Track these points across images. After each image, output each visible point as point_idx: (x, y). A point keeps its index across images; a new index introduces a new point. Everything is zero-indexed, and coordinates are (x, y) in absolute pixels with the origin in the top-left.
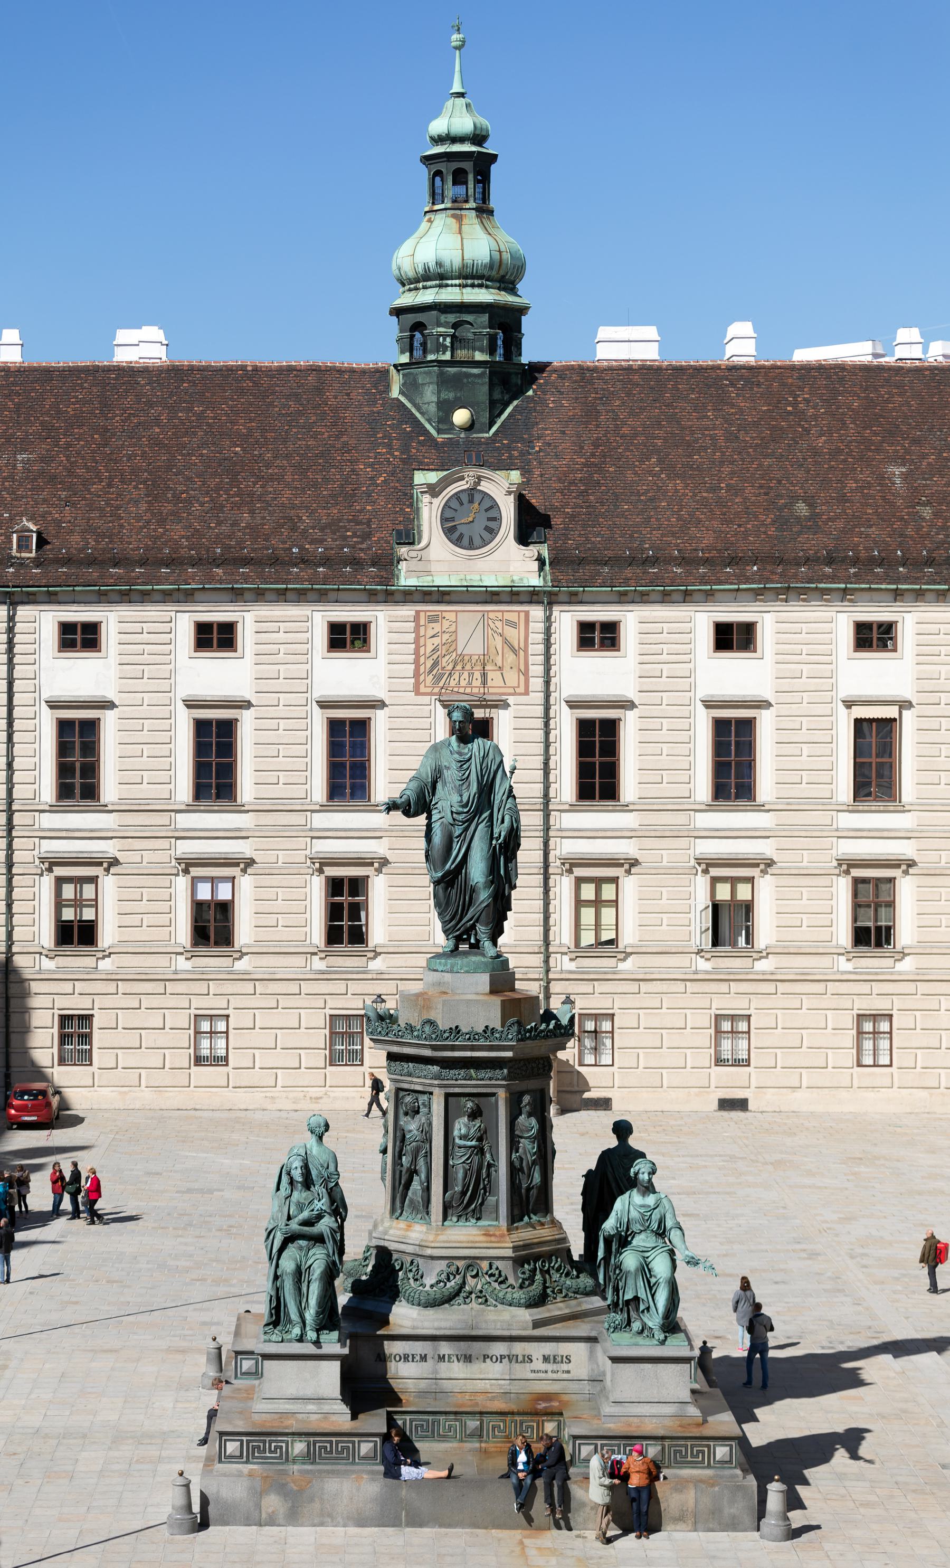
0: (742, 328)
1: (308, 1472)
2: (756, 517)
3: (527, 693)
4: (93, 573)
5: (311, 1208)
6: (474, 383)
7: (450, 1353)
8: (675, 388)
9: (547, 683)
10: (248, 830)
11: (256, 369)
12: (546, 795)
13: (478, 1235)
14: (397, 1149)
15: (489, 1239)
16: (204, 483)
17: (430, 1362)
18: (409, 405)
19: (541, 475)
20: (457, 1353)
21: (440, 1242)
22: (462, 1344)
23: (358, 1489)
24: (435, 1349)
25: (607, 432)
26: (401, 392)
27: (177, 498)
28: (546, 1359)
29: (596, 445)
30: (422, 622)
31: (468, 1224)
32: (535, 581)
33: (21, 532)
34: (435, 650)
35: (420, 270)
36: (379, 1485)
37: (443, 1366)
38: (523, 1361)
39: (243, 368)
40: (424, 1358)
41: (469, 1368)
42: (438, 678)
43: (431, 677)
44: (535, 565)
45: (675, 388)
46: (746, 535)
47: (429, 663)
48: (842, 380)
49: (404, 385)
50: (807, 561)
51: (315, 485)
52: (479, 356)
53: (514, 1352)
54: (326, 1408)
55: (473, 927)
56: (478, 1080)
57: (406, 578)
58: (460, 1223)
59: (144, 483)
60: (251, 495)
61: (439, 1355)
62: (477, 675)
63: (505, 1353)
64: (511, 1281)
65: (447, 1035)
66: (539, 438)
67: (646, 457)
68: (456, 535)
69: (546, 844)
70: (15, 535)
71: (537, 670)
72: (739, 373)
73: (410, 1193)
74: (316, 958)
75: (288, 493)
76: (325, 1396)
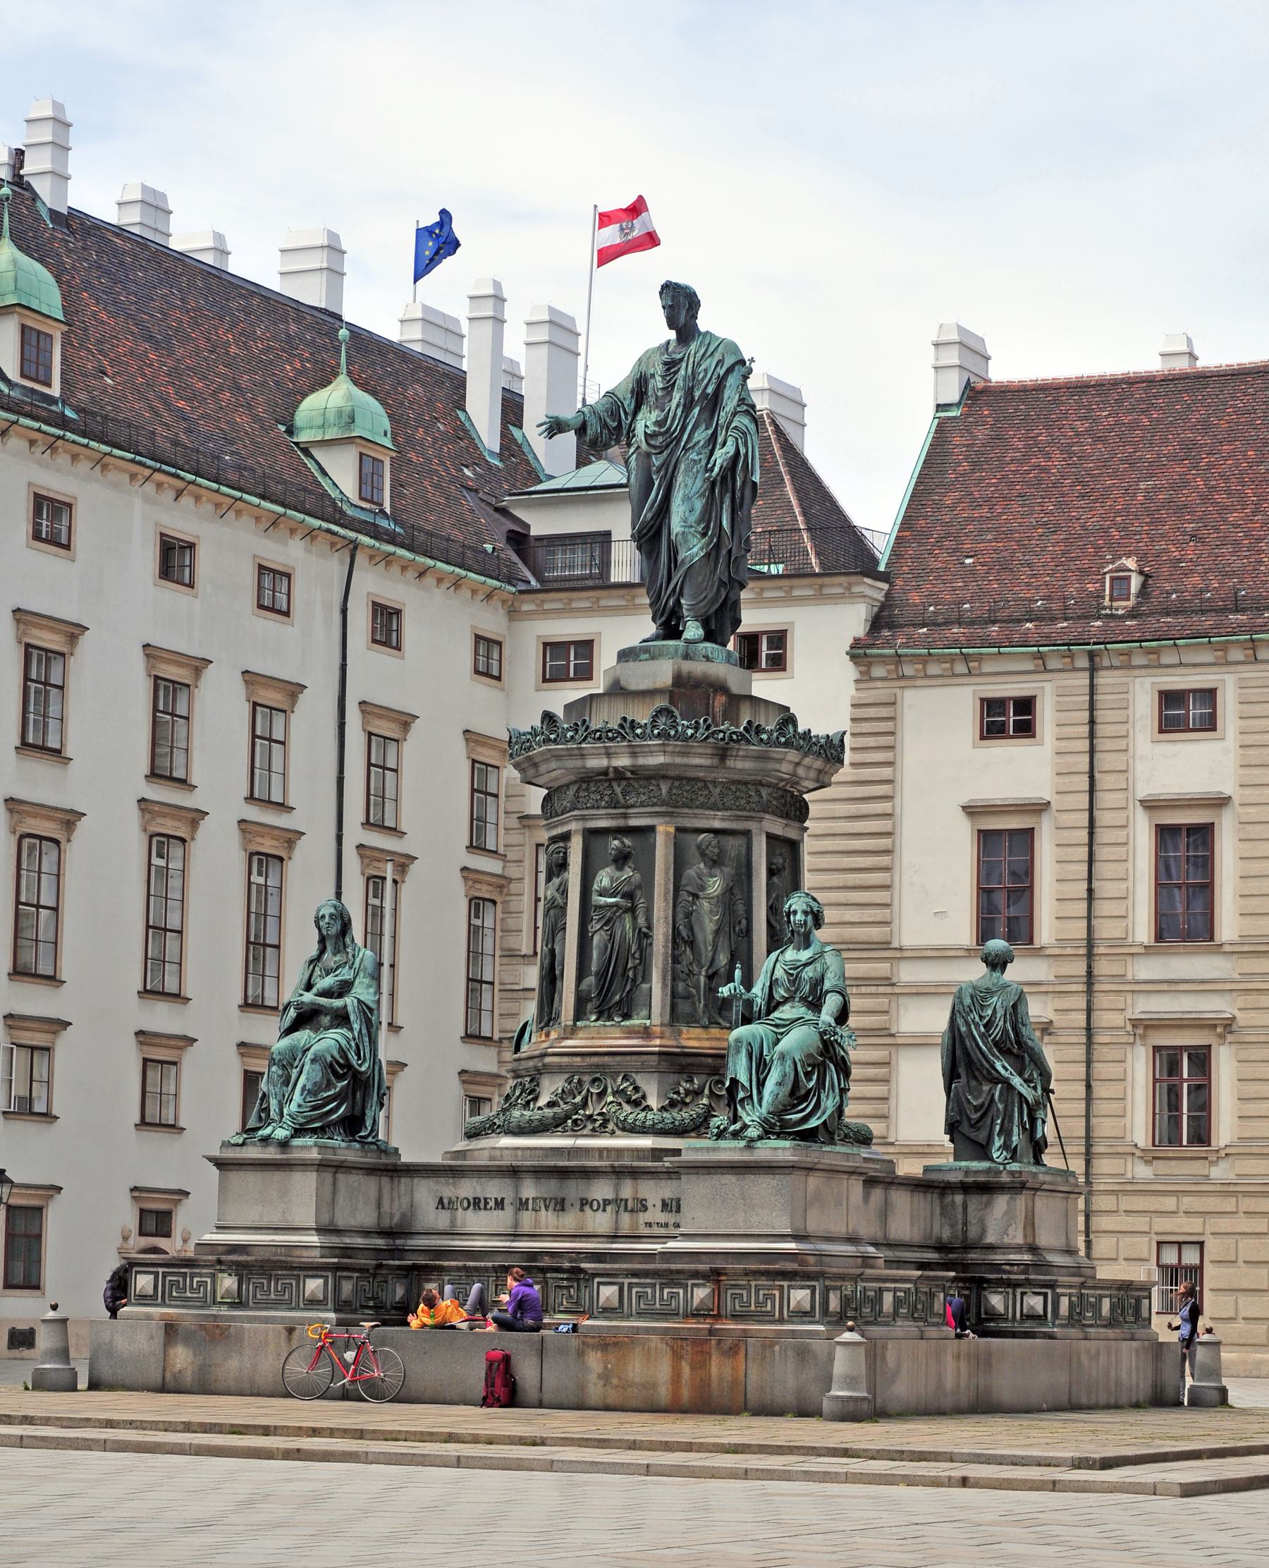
4: (1208, 621)
20: (545, 1196)
24: (517, 1191)
31: (608, 1023)
33: (1116, 571)
40: (500, 1204)
41: (561, 1219)
55: (678, 603)
58: (600, 1022)
61: (520, 1199)
63: (610, 1196)
64: (653, 1101)
65: (570, 734)
70: (1108, 577)
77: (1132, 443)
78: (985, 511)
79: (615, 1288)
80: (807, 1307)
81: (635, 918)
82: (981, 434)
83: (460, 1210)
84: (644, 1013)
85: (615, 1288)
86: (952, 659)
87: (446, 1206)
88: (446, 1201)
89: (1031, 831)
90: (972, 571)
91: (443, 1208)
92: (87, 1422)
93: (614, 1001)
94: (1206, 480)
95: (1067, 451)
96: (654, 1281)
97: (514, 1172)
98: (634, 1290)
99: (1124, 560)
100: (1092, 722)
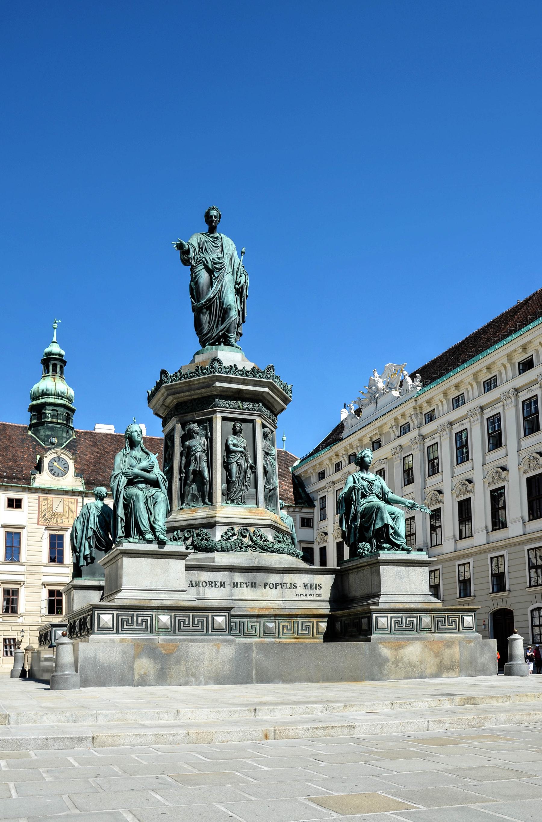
5: (148, 461)
6: (57, 430)
7: (241, 581)
13: (245, 512)
14: (184, 462)
15: (253, 514)
17: (228, 588)
18: (35, 437)
19: (80, 460)
20: (246, 581)
21: (222, 514)
23: (217, 652)
24: (231, 578)
28: (305, 586)
36: (234, 649)
37: (237, 591)
40: (223, 585)
44: (80, 484)
53: (285, 582)
54: (176, 596)
56: (243, 410)
58: (233, 505)
61: (234, 583)
63: (279, 582)
66: (79, 450)
68: (53, 472)
79: (386, 618)
83: (202, 587)
85: (386, 618)
87: (194, 585)
88: (194, 583)
91: (192, 586)
93: (238, 496)
96: (402, 615)
97: (231, 569)
98: (393, 620)
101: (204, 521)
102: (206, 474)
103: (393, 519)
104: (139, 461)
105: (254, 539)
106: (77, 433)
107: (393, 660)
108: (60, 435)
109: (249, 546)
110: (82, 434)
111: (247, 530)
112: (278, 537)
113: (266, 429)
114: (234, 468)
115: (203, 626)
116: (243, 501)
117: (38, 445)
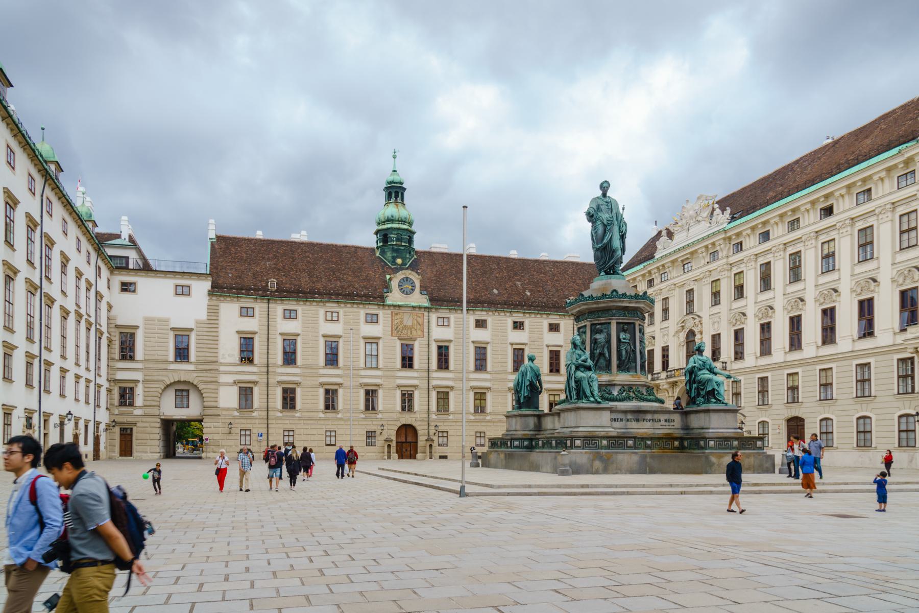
0: (473, 245)
1: (608, 452)
2: (484, 292)
3: (423, 337)
8: (456, 259)
9: (429, 334)
10: (342, 375)
11: (336, 246)
12: (429, 367)
14: (592, 347)
16: (325, 273)
17: (624, 422)
22: (636, 415)
25: (439, 269)
26: (380, 254)
27: (317, 277)
28: (666, 421)
29: (437, 271)
30: (393, 315)
32: (427, 304)
34: (397, 324)
35: (386, 218)
38: (658, 421)
39: (332, 245)
40: (621, 420)
42: (398, 332)
43: (396, 332)
45: (456, 259)
46: (482, 297)
47: (395, 327)
48: (500, 260)
49: (380, 252)
50: (500, 304)
51: (358, 276)
52: (403, 244)
57: (389, 302)
59: (307, 272)
60: (340, 277)
62: (409, 331)
67: (451, 275)
68: (403, 290)
69: (429, 381)
71: (426, 330)
72: (472, 257)
73: (598, 364)
74: (362, 414)
75: (350, 278)
76: (605, 425)
77: (262, 254)
78: (230, 264)
80: (761, 446)
81: (630, 346)
82: (223, 246)
84: (634, 370)
86: (234, 297)
89: (253, 338)
90: (231, 277)
92: (649, 486)
94: (283, 264)
95: (245, 253)
97: (625, 412)
99: (272, 279)
100: (268, 315)
101: (608, 383)
102: (607, 355)
103: (717, 385)
104: (580, 356)
105: (636, 393)
106: (417, 253)
107: (717, 463)
108: (404, 256)
109: (633, 398)
110: (422, 254)
111: (632, 388)
112: (648, 391)
113: (641, 326)
114: (624, 353)
115: (622, 445)
116: (628, 370)
117: (386, 265)
